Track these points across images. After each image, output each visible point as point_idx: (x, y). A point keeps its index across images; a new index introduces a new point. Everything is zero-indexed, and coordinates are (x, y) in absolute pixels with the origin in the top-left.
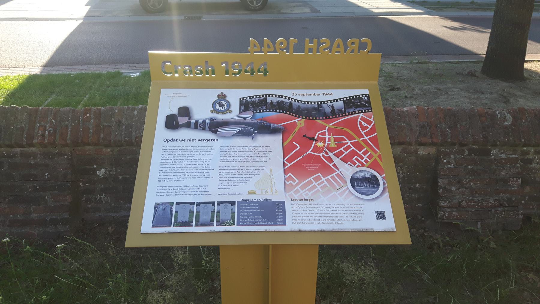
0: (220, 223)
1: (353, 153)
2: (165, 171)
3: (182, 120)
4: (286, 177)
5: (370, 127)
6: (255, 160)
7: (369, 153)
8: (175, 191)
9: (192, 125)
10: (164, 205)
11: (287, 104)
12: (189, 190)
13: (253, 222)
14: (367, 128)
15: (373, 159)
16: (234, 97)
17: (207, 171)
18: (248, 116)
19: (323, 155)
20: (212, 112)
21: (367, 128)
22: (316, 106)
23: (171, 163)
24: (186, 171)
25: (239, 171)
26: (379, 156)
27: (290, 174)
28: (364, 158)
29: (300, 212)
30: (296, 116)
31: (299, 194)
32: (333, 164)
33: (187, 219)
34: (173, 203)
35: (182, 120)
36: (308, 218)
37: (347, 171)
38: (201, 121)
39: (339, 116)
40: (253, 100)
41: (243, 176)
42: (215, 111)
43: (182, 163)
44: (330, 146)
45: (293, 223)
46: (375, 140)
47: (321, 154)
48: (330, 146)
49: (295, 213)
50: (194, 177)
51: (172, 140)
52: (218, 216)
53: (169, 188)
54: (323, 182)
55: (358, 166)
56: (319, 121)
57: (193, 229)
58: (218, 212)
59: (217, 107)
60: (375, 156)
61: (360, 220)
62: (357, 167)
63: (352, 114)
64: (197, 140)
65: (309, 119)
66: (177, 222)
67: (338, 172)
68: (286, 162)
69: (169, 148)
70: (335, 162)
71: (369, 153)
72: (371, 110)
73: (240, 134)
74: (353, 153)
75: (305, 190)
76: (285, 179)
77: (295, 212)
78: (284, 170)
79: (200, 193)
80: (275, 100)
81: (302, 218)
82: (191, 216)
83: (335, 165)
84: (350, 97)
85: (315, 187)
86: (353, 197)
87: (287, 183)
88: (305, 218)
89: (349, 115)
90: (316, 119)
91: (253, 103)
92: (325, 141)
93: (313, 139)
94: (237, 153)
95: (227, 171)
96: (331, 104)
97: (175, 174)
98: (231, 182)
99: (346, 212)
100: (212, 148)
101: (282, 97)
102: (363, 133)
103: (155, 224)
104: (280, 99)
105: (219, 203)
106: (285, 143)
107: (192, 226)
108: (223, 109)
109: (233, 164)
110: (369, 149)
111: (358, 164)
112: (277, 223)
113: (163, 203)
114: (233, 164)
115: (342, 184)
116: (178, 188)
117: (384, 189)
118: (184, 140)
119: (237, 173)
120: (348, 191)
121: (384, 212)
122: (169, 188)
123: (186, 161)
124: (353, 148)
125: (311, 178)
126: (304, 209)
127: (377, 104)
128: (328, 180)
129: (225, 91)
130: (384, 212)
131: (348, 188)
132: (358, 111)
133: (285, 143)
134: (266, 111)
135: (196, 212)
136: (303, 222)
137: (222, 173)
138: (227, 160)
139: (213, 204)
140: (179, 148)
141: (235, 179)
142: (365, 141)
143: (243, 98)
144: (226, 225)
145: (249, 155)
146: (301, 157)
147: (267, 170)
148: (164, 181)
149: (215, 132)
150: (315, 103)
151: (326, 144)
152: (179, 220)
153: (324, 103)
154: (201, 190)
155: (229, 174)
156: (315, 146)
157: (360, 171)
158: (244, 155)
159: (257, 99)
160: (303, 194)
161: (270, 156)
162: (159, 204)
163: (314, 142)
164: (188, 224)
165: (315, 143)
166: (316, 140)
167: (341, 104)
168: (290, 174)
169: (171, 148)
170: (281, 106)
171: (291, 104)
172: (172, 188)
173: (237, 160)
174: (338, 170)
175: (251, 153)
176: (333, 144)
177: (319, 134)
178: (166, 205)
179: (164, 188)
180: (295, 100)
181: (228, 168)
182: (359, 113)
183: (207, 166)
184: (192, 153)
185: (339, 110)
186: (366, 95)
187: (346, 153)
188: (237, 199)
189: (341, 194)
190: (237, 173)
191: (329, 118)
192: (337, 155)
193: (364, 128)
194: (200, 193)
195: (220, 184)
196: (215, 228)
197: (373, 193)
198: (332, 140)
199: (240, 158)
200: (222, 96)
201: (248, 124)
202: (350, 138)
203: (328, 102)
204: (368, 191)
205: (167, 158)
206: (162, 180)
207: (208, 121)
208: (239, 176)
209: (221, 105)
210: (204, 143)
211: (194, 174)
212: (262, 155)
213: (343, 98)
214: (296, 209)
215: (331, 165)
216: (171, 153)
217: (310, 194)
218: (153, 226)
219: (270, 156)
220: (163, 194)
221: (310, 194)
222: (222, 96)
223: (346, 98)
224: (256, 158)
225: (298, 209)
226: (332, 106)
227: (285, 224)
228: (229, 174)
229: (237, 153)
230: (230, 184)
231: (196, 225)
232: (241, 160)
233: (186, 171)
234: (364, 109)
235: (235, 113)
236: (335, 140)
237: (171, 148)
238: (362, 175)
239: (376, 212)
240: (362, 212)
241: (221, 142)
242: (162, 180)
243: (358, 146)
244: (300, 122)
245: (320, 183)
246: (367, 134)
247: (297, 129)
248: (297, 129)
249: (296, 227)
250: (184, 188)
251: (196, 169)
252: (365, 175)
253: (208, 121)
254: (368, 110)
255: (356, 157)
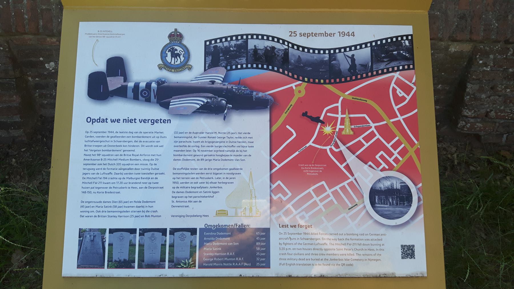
0: (175, 264)
1: (378, 146)
2: (91, 176)
3: (114, 83)
4: (274, 186)
5: (408, 98)
6: (227, 158)
7: (403, 146)
8: (106, 209)
9: (130, 93)
10: (92, 233)
11: (281, 53)
12: (128, 209)
13: (222, 262)
14: (404, 99)
15: (407, 157)
16: (197, 36)
17: (154, 176)
18: (218, 75)
19: (331, 150)
20: (160, 68)
21: (404, 99)
22: (327, 57)
23: (100, 162)
24: (122, 176)
25: (202, 176)
26: (417, 152)
27: (279, 182)
28: (393, 154)
29: (292, 247)
30: (293, 77)
31: (291, 216)
32: (344, 164)
33: (125, 256)
34: (105, 230)
35: (114, 83)
36: (302, 257)
37: (367, 177)
38: (143, 85)
39: (362, 78)
40: (226, 44)
41: (209, 185)
42: (166, 66)
43: (115, 162)
44: (343, 133)
45: (280, 264)
46: (412, 122)
47: (328, 148)
48: (343, 133)
49: (283, 249)
50: (134, 185)
51: (99, 120)
52: (171, 252)
53: (99, 205)
54: (328, 196)
55: (383, 170)
56: (329, 87)
57: (136, 272)
58: (172, 246)
59: (169, 58)
60: (411, 152)
61: (377, 260)
62: (381, 170)
63: (383, 73)
64: (137, 121)
65: (314, 82)
66: (112, 261)
67: (352, 179)
68: (274, 162)
69: (95, 135)
70: (348, 161)
71: (403, 146)
72: (414, 66)
73: (206, 110)
74: (378, 146)
75: (300, 210)
76: (271, 191)
77: (283, 246)
78: (271, 176)
79: (144, 214)
80: (262, 44)
81: (293, 257)
82: (132, 252)
83: (347, 167)
84: (381, 40)
85: (315, 204)
86: (371, 222)
87: (275, 198)
88: (298, 257)
89: (378, 74)
90: (325, 83)
91: (226, 51)
92: (335, 125)
93: (317, 120)
94: (199, 144)
95: (184, 176)
96: (350, 54)
97: (106, 181)
98: (190, 195)
99: (358, 247)
100: (161, 135)
101: (273, 40)
102: (396, 108)
103: (83, 262)
104: (269, 44)
105: (173, 231)
106: (275, 128)
107: (134, 268)
108: (179, 62)
109: (194, 164)
110: (403, 140)
111: (384, 165)
112: (258, 264)
113: (90, 230)
114: (194, 164)
115: (357, 200)
116: (112, 204)
117: (418, 208)
118: (118, 121)
119: (200, 181)
120: (364, 212)
121: (413, 246)
122: (99, 205)
123: (122, 157)
124: (378, 136)
125: (311, 190)
126: (298, 241)
127: (423, 55)
128: (335, 193)
129: (182, 27)
130: (413, 246)
131: (365, 207)
132: (393, 68)
133: (275, 128)
134: (247, 68)
135: (139, 245)
136: (295, 262)
137: (176, 180)
138: (185, 158)
139: (163, 231)
140: (111, 135)
141: (197, 190)
142: (398, 124)
143: (210, 41)
144: (182, 267)
145: (218, 149)
146: (297, 153)
147: (245, 175)
148: (90, 192)
149: (166, 106)
150: (324, 50)
151: (337, 130)
152: (115, 258)
153: (340, 52)
154: (145, 209)
155: (187, 181)
156: (321, 132)
157: (386, 178)
158: (211, 149)
159: (233, 43)
160: (298, 217)
161: (250, 151)
162: (85, 231)
163: (320, 124)
164: (128, 264)
165: (321, 128)
166: (322, 122)
167: (367, 52)
168: (279, 182)
169: (98, 135)
170: (270, 58)
171: (286, 52)
172: (103, 204)
173: (200, 158)
174: (352, 175)
175: (222, 144)
176: (348, 131)
177: (328, 111)
178: (96, 233)
179: (91, 204)
180: (293, 45)
181: (187, 171)
182: (393, 71)
183: (154, 167)
184: (130, 144)
185: (362, 65)
186: (407, 36)
187: (367, 145)
188: (198, 224)
189: (354, 217)
190: (200, 181)
191: (346, 81)
192: (352, 150)
193: (399, 100)
194: (144, 214)
195: (174, 199)
196: (168, 272)
197: (402, 214)
198: (347, 122)
199: (205, 153)
200: (176, 37)
201: (218, 92)
202: (376, 118)
203: (345, 51)
204: (394, 212)
205: (93, 153)
206: (87, 190)
207: (154, 85)
208: (202, 185)
209: (175, 55)
210: (148, 127)
211: (135, 181)
212: (239, 149)
213: (371, 43)
214: (285, 241)
215: (342, 167)
216: (99, 144)
217: (307, 216)
218: (79, 267)
219: (250, 151)
220: (90, 214)
221: (307, 216)
222: (176, 37)
223: (376, 41)
224: (229, 153)
225: (288, 241)
226: (352, 58)
227: (268, 266)
228: (187, 181)
229: (199, 144)
230: (188, 199)
231: (140, 267)
232: (207, 158)
233: (122, 176)
234: (403, 63)
235: (196, 72)
236: (352, 121)
237: (98, 135)
238: (387, 184)
239: (402, 246)
240: (382, 247)
241: (176, 124)
242: (87, 190)
243: (385, 131)
244: (299, 88)
245: (321, 196)
246: (402, 111)
247: (293, 102)
248: (293, 102)
249: (284, 271)
250: (121, 204)
251: (137, 171)
252: (392, 185)
253: (154, 85)
254: (409, 66)
255: (382, 152)
